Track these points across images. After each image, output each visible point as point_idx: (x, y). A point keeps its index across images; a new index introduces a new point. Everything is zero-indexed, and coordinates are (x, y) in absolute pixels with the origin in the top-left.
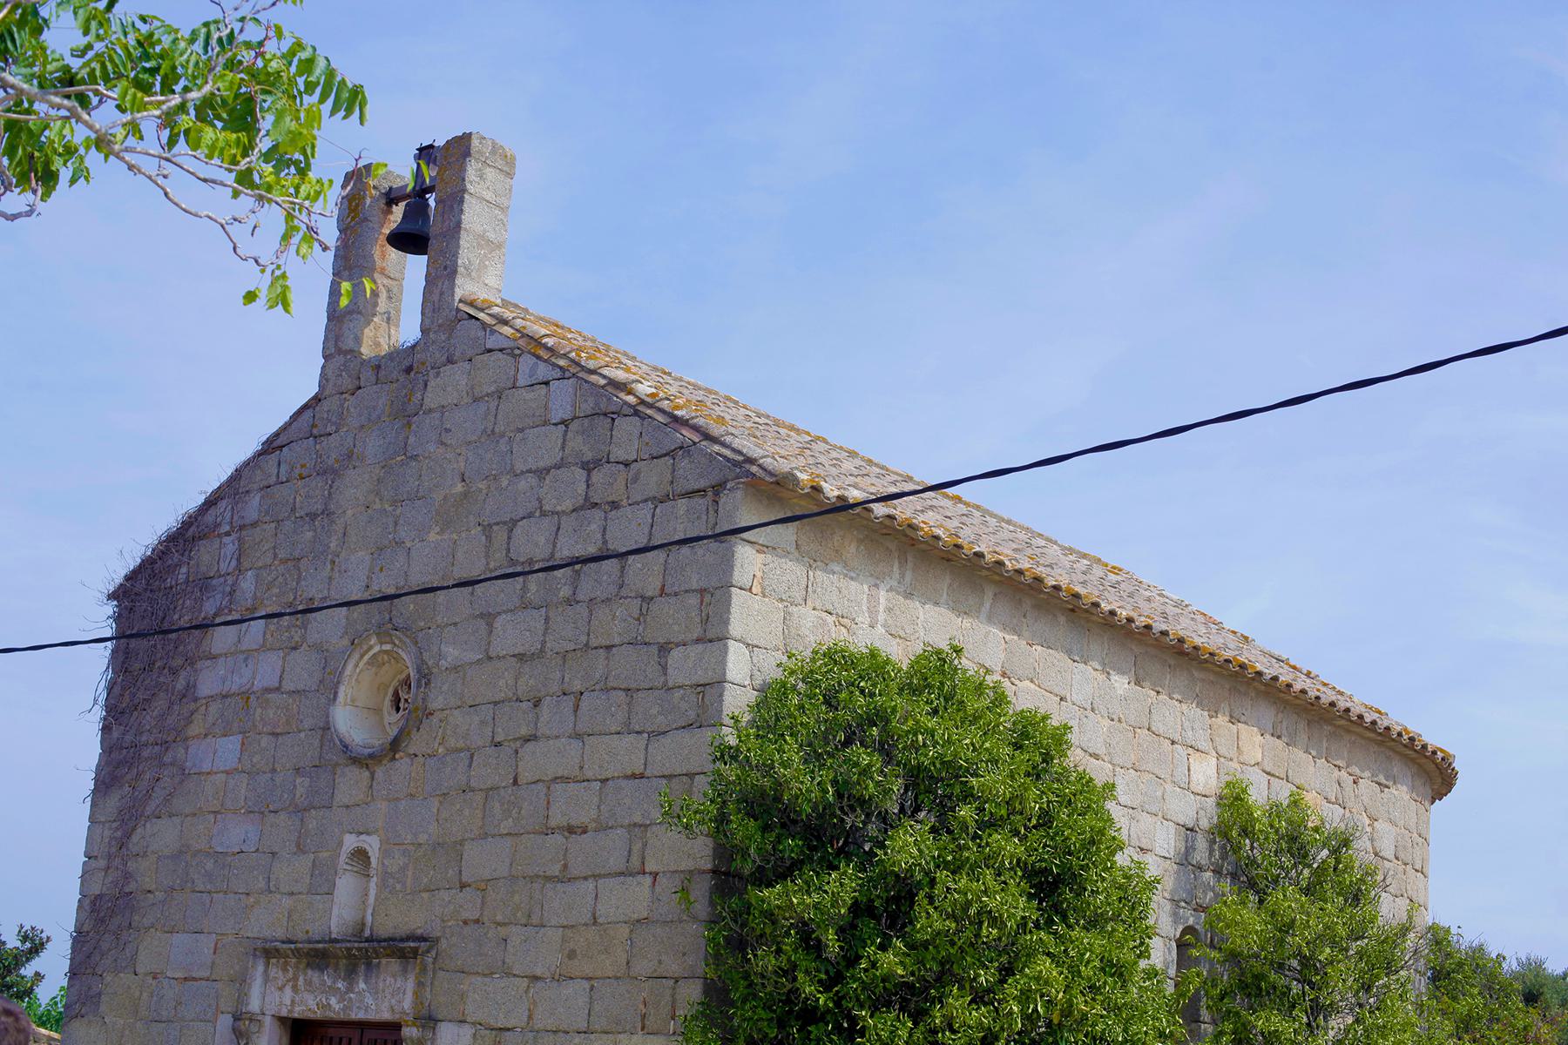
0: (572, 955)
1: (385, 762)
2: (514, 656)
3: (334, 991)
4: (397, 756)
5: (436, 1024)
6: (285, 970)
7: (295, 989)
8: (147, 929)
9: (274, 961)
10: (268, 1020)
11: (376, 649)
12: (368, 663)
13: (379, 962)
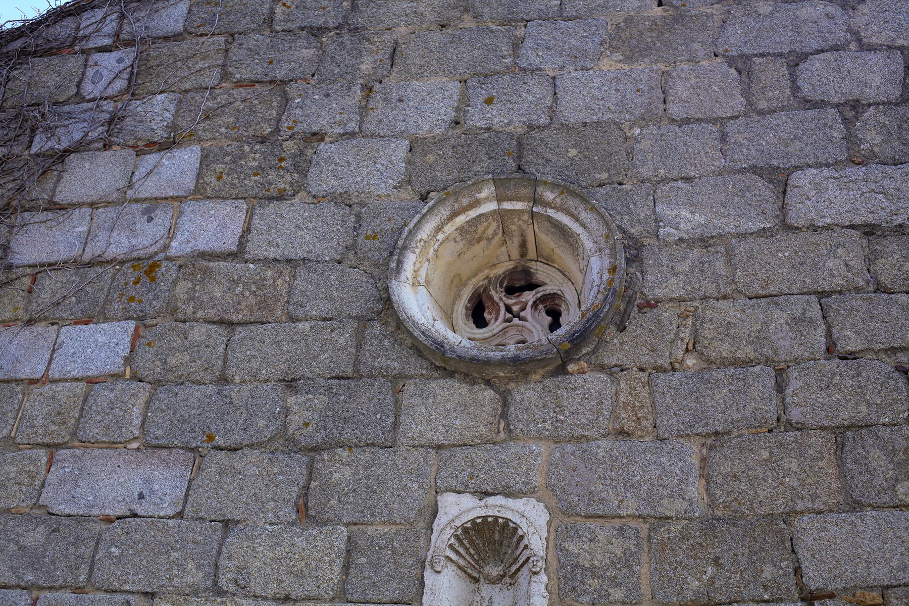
1: (537, 377)
2: (852, 227)
4: (571, 367)
11: (492, 206)
12: (461, 230)
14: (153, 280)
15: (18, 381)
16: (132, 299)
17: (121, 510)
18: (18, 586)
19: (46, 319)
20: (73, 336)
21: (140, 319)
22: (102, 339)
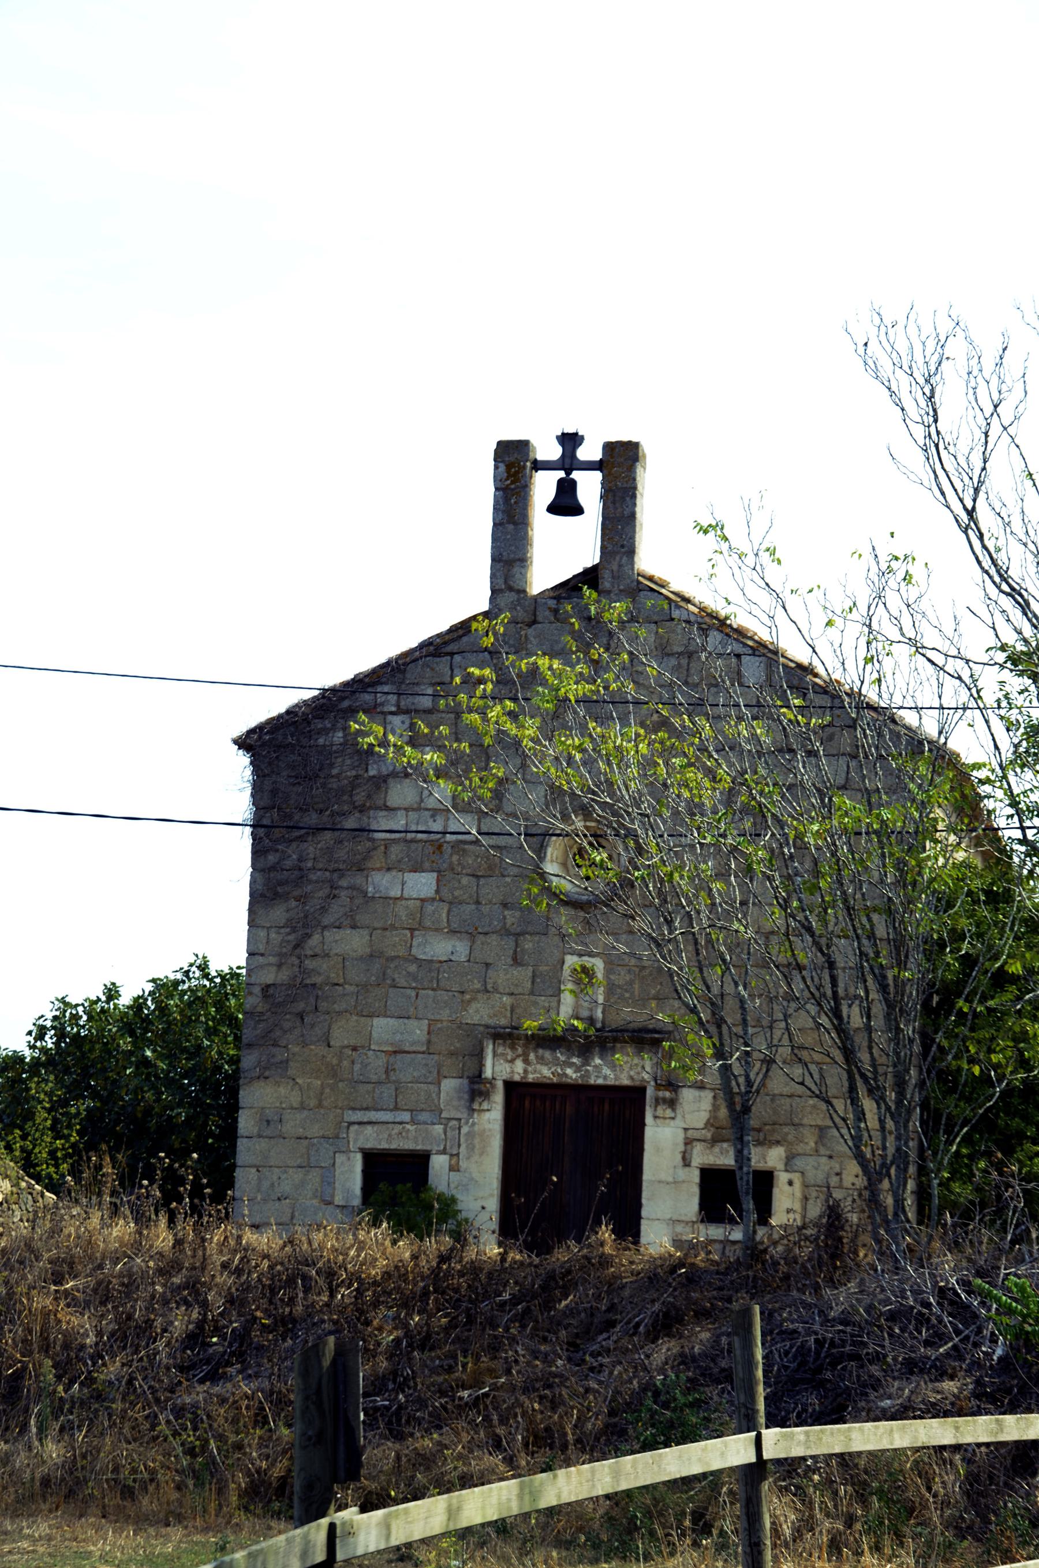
3: (571, 1065)
5: (676, 1091)
6: (513, 1048)
7: (526, 1061)
8: (339, 1013)
9: (501, 1041)
10: (500, 1085)
13: (614, 1047)
15: (390, 898)
17: (445, 958)
20: (411, 878)
21: (439, 872)
22: (424, 881)
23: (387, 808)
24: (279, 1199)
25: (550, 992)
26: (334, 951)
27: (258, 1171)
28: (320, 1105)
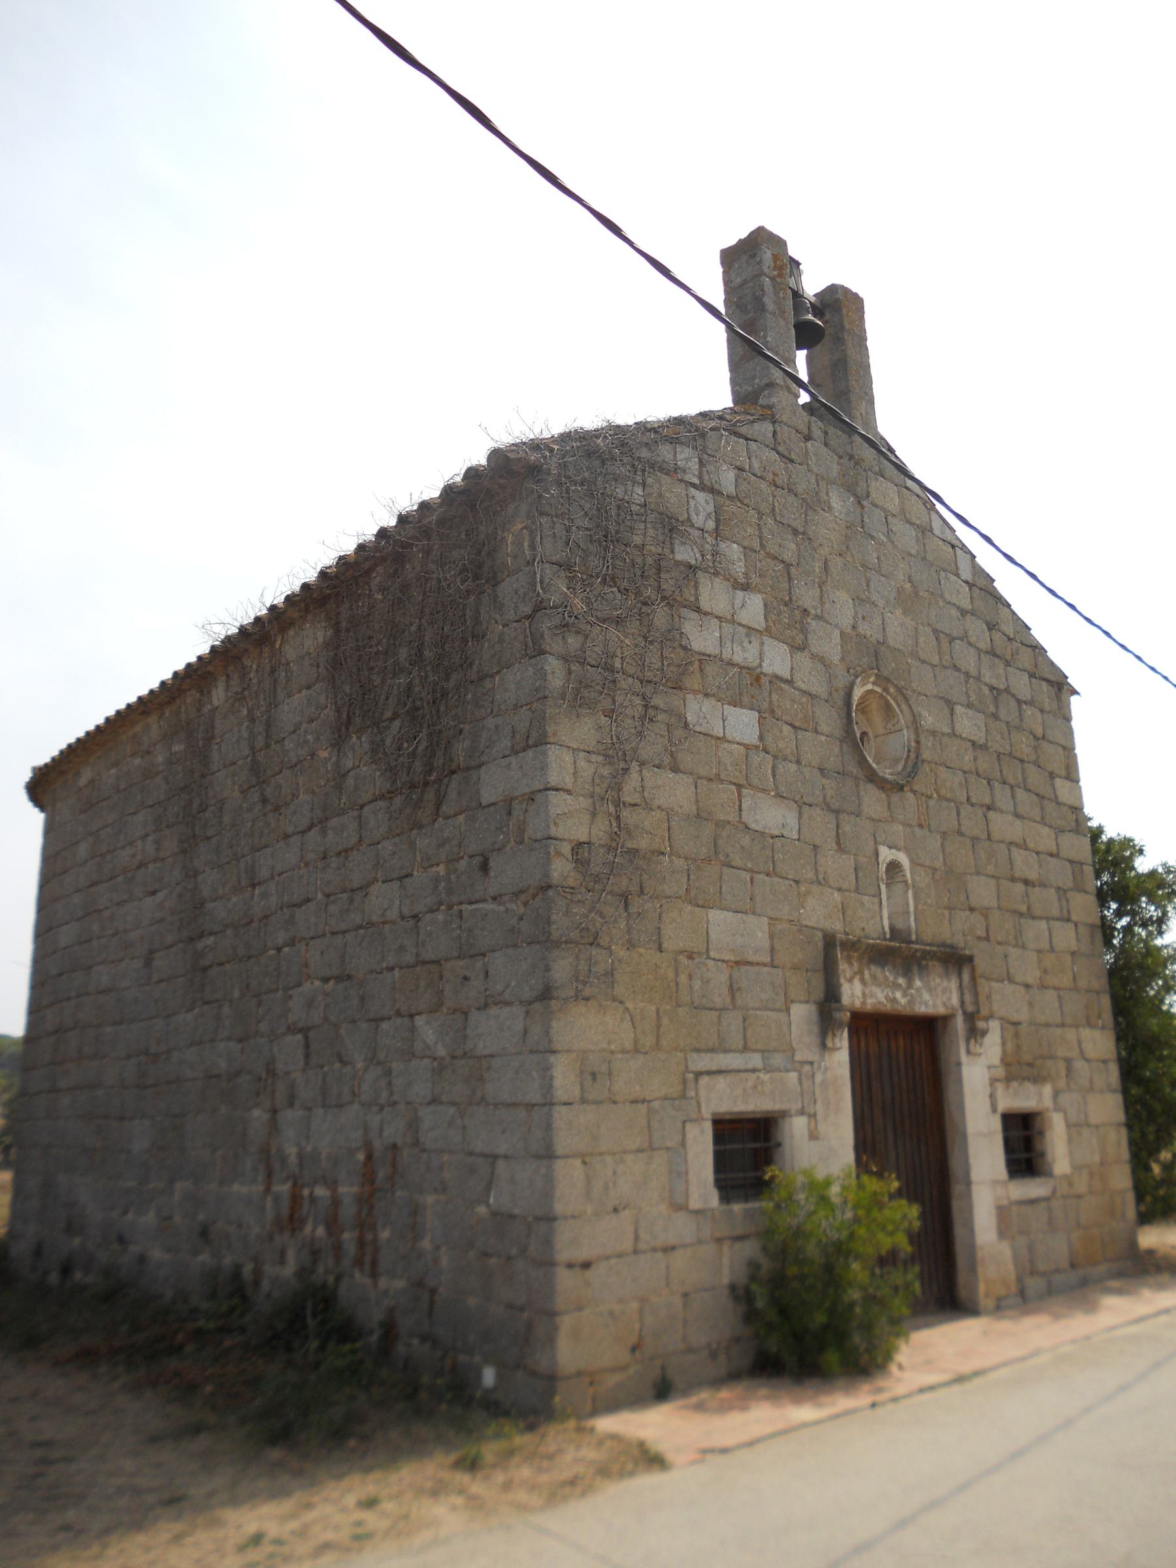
0: (1045, 971)
3: (897, 986)
6: (850, 964)
13: (927, 965)
14: (760, 686)
16: (753, 697)
17: (776, 832)
18: (744, 870)
19: (714, 695)
23: (698, 610)
24: (615, 1210)
25: (872, 892)
26: (657, 802)
27: (584, 1163)
28: (658, 1046)
